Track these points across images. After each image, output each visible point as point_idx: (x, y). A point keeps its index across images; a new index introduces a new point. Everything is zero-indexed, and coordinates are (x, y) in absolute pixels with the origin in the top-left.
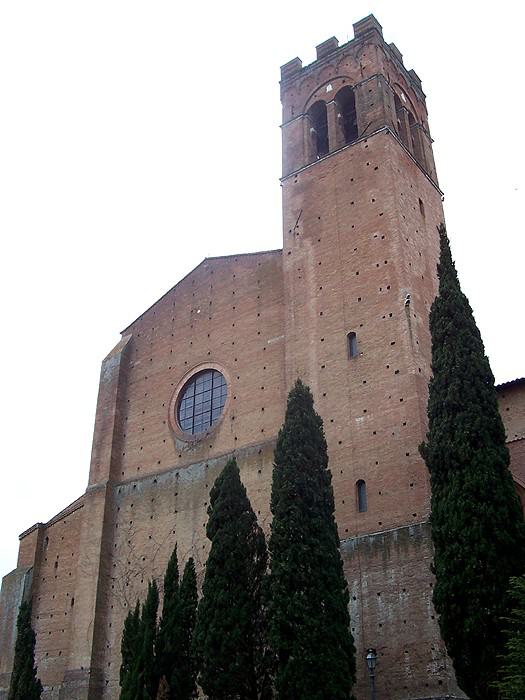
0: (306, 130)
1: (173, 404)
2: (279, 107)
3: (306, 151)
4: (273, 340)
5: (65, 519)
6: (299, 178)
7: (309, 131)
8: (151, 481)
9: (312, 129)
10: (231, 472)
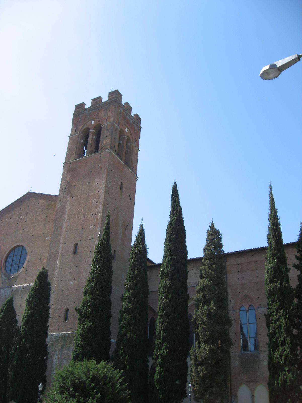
0: (79, 141)
2: (70, 126)
3: (77, 151)
4: (48, 238)
6: (71, 165)
7: (80, 141)
9: (82, 141)
10: (10, 303)
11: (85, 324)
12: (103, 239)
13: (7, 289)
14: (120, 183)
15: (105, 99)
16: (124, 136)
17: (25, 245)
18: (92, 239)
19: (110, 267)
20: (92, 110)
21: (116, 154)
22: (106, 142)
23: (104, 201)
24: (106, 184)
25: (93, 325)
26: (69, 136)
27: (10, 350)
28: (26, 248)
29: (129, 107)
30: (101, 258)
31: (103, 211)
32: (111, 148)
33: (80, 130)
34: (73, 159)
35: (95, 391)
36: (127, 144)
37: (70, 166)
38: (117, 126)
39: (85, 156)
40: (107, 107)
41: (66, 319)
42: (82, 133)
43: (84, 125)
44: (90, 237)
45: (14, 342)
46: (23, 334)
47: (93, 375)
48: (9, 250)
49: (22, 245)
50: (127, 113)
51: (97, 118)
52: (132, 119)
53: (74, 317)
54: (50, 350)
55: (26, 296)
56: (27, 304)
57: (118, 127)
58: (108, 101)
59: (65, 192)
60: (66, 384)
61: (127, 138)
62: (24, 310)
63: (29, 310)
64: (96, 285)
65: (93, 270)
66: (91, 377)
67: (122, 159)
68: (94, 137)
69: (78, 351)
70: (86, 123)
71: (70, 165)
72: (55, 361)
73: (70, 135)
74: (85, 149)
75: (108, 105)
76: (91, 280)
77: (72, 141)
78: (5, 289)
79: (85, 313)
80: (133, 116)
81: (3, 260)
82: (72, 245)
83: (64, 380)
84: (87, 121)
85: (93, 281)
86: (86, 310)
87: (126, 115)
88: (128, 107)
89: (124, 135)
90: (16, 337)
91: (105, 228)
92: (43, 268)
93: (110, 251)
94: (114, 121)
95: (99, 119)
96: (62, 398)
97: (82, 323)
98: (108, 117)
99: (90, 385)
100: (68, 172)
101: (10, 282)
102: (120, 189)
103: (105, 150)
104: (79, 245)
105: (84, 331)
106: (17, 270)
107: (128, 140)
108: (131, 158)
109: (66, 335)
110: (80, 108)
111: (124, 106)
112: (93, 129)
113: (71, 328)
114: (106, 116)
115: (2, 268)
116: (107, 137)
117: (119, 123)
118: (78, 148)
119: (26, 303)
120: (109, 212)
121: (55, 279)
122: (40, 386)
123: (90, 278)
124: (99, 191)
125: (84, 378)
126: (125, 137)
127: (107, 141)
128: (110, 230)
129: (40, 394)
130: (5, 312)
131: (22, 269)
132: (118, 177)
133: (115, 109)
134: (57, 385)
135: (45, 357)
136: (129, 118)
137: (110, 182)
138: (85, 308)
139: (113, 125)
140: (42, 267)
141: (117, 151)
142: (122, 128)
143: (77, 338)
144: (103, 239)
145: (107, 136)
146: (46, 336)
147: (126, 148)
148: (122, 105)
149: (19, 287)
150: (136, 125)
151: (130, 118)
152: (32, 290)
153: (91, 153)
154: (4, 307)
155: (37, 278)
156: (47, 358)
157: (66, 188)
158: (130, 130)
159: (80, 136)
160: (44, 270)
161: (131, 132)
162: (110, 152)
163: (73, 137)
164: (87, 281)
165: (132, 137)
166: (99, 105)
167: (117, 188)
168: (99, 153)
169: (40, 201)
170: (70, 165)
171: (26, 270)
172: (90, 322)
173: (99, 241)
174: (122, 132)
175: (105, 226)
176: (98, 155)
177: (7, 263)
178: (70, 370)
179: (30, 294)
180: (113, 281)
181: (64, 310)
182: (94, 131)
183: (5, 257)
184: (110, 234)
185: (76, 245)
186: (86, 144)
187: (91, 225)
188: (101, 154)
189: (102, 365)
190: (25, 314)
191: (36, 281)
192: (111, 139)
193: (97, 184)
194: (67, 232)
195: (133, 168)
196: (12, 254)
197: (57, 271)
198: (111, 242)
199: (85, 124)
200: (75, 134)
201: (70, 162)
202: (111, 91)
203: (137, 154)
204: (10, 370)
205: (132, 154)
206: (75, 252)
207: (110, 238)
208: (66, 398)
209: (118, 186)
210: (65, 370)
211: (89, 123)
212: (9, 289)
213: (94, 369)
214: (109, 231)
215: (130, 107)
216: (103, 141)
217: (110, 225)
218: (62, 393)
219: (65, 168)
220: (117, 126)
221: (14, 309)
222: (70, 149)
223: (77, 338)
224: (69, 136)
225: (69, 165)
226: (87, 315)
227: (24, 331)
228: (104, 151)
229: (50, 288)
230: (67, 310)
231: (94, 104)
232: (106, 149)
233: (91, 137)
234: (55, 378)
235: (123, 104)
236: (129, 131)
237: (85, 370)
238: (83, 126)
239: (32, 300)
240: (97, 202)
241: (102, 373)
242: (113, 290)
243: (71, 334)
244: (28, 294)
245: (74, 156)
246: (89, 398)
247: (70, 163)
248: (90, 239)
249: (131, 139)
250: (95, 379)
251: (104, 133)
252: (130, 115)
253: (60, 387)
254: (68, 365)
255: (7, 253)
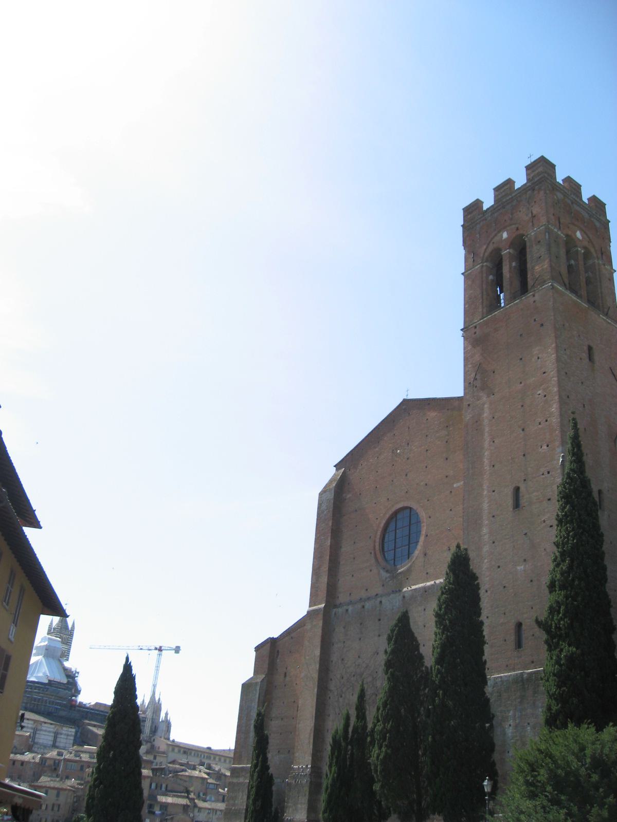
1: (378, 537)
2: (461, 252)
4: (459, 484)
5: (293, 635)
6: (477, 330)
8: (359, 606)
9: (491, 277)
10: (404, 621)
11: (561, 650)
12: (571, 470)
13: (392, 596)
14: (586, 348)
15: (520, 180)
16: (576, 249)
17: (414, 506)
18: (548, 473)
19: (596, 527)
20: (499, 210)
21: (567, 289)
22: (541, 269)
23: (559, 391)
24: (557, 356)
25: (579, 652)
26: (462, 274)
27: (416, 715)
28: (417, 511)
29: (574, 186)
30: (574, 509)
31: (560, 412)
32: (553, 278)
33: (482, 255)
34: (480, 317)
35: (601, 790)
36: (585, 264)
37: (475, 333)
38: (556, 230)
39: (503, 307)
40: (528, 196)
41: (519, 644)
42: (486, 262)
43: (488, 244)
44: (542, 470)
45: (421, 698)
46: (437, 682)
47: (593, 757)
48: (386, 520)
49: (409, 505)
50: (574, 199)
51: (511, 225)
52: (587, 209)
53: (536, 638)
54: (496, 708)
55: (433, 605)
56: (436, 622)
57: (559, 233)
58: (528, 184)
59: (476, 387)
60: (539, 778)
61: (583, 251)
62: (433, 633)
63: (443, 633)
64: (570, 567)
65: (561, 538)
66: (588, 760)
67: (580, 297)
68: (514, 264)
69: (555, 708)
70: (492, 238)
71: (475, 330)
72: (510, 731)
73: (463, 271)
74: (500, 293)
75: (530, 192)
76: (559, 559)
77: (470, 283)
78: (391, 597)
79: (556, 627)
80: (587, 202)
81: (378, 540)
82: (509, 491)
83: (533, 770)
84: (493, 234)
85: (564, 561)
86: (559, 621)
87: (572, 203)
88: (573, 186)
89: (576, 246)
90: (425, 689)
91: (569, 445)
92: (458, 546)
93: (590, 494)
94: (548, 222)
95: (517, 226)
96: (535, 806)
97: (555, 648)
98: (534, 216)
99: (590, 777)
100: (474, 347)
101: (397, 581)
102: (588, 360)
103: (541, 287)
104: (522, 489)
105: (561, 665)
106: (407, 556)
107: (587, 255)
108: (599, 291)
109: (525, 676)
110: (473, 211)
111: (564, 187)
112: (509, 248)
113: (533, 662)
114: (530, 215)
115: (378, 556)
116: (540, 257)
117: (559, 222)
118: (485, 293)
119: (434, 619)
120: (573, 413)
121: (485, 564)
122: (485, 783)
123: (558, 554)
124: (544, 373)
125: (575, 764)
126: (579, 249)
127: (542, 266)
128: (583, 448)
129: (489, 800)
130: (396, 642)
131: (416, 552)
132: (579, 336)
133: (545, 196)
134: (521, 779)
135: (487, 725)
136: (578, 208)
137: (565, 350)
138: (555, 618)
139: (548, 230)
140: (455, 545)
141: (567, 283)
142: (570, 233)
143: (548, 680)
144: (571, 470)
145: (541, 256)
146: (484, 681)
147: (586, 272)
148: (557, 184)
149: (415, 589)
150: (596, 219)
151: (581, 208)
152: (443, 593)
153: (512, 298)
154: (392, 631)
155: (449, 567)
156: (492, 726)
157: (475, 379)
158: (585, 232)
159: (484, 268)
160: (460, 549)
161: (588, 237)
162: (553, 287)
163: (471, 273)
164: (550, 561)
165: (594, 247)
166: (510, 197)
167: (581, 359)
168: (531, 294)
169: (429, 413)
170: (475, 331)
171: (425, 555)
172: (570, 645)
173: (563, 475)
174: (570, 242)
175: (569, 442)
176: (528, 299)
177: (386, 545)
178: (543, 747)
179: (439, 600)
180: (607, 555)
181: (512, 626)
182: (511, 251)
183: (379, 533)
184: (585, 458)
185: (517, 489)
186: (499, 282)
187: (539, 444)
188: (534, 296)
189: (610, 734)
190: (435, 641)
191: (447, 574)
192: (550, 260)
193: (538, 358)
194: (493, 466)
195: (608, 310)
196: (392, 527)
197: (486, 549)
198: (589, 474)
199: (490, 242)
200: (474, 266)
201: (474, 325)
202: (529, 163)
203: (611, 280)
204: (424, 754)
205: (600, 282)
206: (517, 505)
207: (584, 466)
208: (544, 807)
209: (584, 354)
210: (532, 749)
211: (496, 239)
212: (397, 594)
213: (593, 743)
214: (581, 451)
215: (576, 185)
216: (533, 268)
217: (580, 439)
218: (532, 796)
219: (465, 338)
220: (556, 230)
221: (413, 634)
222: (470, 299)
223: (548, 680)
224: (462, 274)
225: (474, 331)
226: (563, 632)
227: (439, 675)
228: (540, 288)
229: (478, 584)
230: (519, 625)
231: (500, 196)
232: (544, 282)
233: (508, 266)
234: (515, 766)
235: (561, 182)
236: (585, 236)
237: (576, 748)
238: (487, 247)
239: (446, 613)
240: (545, 396)
241: (611, 751)
242: (608, 573)
243: (534, 672)
244: (437, 602)
245: (480, 310)
246: (592, 806)
247: (475, 327)
248: (543, 474)
249: (592, 250)
250: (599, 764)
251: (534, 252)
252: (582, 203)
253: (527, 783)
254: (537, 739)
255: (382, 525)
